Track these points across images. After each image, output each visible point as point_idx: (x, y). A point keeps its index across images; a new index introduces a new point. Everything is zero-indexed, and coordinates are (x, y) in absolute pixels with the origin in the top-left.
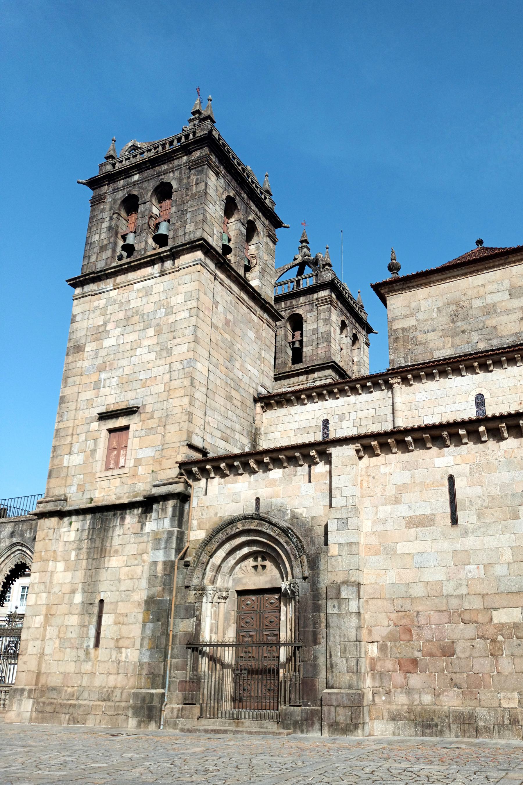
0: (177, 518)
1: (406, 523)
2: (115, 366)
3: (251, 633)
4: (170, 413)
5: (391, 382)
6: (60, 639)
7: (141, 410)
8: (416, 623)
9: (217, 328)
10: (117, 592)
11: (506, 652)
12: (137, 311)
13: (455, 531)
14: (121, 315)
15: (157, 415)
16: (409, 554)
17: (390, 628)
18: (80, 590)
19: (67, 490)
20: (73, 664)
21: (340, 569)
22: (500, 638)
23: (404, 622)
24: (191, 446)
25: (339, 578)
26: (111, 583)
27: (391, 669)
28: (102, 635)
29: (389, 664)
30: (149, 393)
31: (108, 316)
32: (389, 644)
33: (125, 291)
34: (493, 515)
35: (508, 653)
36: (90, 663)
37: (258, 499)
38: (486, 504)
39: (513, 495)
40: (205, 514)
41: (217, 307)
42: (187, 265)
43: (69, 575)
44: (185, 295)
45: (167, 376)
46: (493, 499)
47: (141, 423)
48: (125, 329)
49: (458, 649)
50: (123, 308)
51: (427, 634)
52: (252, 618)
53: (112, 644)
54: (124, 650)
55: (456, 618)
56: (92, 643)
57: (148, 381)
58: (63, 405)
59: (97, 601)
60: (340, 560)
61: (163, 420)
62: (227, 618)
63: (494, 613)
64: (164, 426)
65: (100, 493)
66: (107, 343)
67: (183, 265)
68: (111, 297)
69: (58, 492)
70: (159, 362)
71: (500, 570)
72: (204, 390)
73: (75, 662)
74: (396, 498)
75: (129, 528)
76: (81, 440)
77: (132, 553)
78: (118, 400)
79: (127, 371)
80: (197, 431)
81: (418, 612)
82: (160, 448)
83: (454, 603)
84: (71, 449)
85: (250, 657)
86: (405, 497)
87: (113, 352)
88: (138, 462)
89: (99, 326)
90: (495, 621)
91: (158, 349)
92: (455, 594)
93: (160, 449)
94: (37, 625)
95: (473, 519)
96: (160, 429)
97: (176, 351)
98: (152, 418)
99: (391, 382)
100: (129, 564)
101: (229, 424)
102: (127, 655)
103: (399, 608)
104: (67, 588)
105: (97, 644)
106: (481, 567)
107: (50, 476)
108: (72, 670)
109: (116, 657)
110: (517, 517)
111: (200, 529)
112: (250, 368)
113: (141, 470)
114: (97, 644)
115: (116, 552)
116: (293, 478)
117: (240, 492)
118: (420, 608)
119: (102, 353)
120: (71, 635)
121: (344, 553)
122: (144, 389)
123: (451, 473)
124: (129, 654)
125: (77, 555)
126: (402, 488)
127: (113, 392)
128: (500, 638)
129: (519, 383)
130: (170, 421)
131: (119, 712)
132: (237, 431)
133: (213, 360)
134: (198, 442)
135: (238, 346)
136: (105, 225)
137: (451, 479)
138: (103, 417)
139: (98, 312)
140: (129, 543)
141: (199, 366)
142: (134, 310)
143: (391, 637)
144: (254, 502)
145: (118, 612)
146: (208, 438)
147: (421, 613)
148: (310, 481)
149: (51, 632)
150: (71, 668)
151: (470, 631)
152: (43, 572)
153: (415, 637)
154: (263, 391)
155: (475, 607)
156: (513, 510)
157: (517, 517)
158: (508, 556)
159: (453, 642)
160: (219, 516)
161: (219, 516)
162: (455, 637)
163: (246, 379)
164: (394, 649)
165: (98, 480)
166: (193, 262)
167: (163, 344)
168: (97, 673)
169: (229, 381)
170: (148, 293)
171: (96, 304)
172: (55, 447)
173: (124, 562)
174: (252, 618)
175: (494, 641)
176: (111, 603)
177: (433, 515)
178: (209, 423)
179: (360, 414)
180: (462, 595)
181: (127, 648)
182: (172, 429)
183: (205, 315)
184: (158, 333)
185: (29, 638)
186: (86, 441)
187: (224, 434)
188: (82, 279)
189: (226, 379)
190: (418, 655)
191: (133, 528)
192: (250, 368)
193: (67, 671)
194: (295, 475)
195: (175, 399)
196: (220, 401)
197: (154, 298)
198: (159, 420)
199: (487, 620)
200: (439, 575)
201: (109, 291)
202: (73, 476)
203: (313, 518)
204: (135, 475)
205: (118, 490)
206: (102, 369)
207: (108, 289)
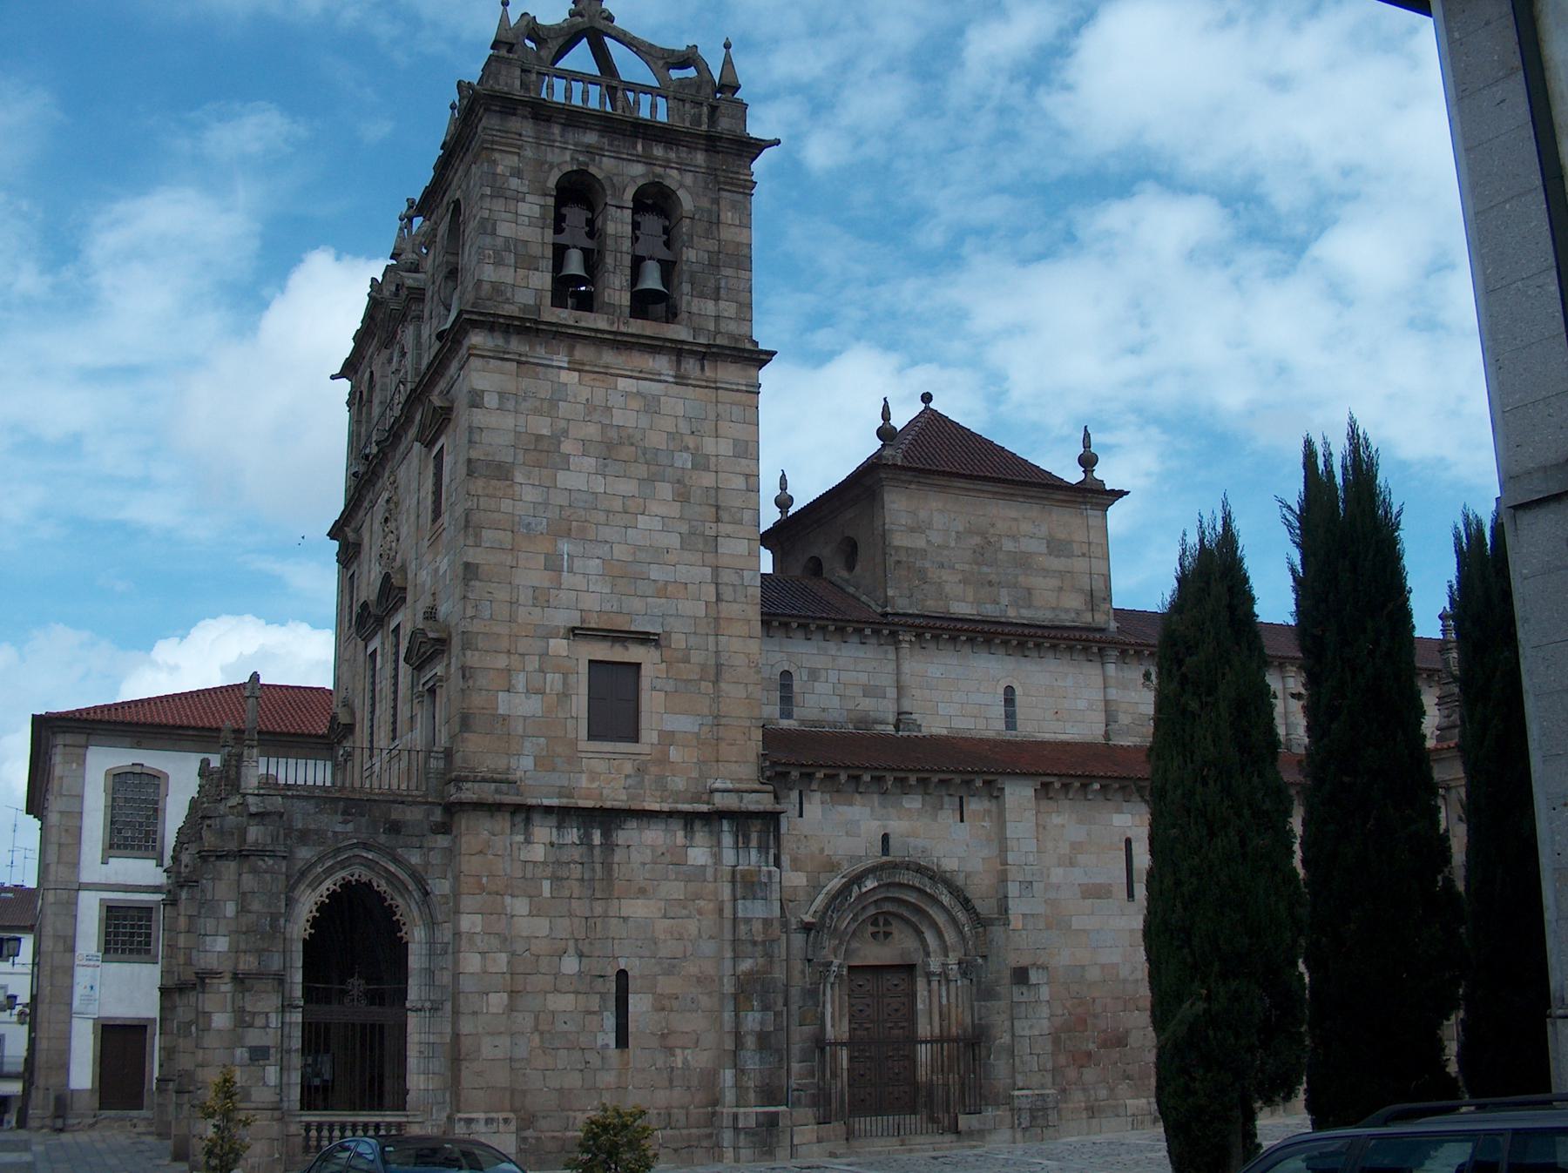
1: (1082, 893)
2: (591, 536)
4: (726, 663)
5: (901, 638)
10: (653, 960)
15: (696, 657)
16: (1084, 931)
18: (571, 950)
19: (513, 763)
20: (577, 1075)
26: (639, 943)
27: (1065, 1064)
30: (673, 612)
32: (1062, 1035)
33: (597, 384)
36: (614, 1073)
37: (885, 838)
42: (735, 387)
48: (606, 466)
49: (1131, 1040)
50: (596, 417)
52: (868, 1005)
54: (678, 1051)
59: (611, 972)
60: (1024, 936)
64: (716, 682)
65: (592, 780)
66: (564, 478)
67: (727, 383)
68: (566, 384)
70: (687, 556)
73: (581, 1071)
74: (1071, 858)
75: (663, 854)
77: (675, 896)
78: (607, 607)
79: (620, 552)
81: (1094, 1001)
84: (510, 681)
85: (868, 1057)
88: (668, 738)
91: (685, 528)
92: (1130, 978)
93: (710, 723)
94: (493, 1010)
97: (726, 547)
99: (901, 638)
100: (672, 915)
102: (686, 1059)
105: (622, 1040)
109: (665, 1062)
113: (674, 754)
114: (622, 1040)
116: (940, 812)
117: (858, 821)
122: (663, 600)
123: (1129, 835)
124: (689, 1058)
126: (1076, 847)
129: (1055, 683)
131: (692, 1143)
137: (1128, 842)
140: (666, 879)
145: (659, 991)
147: (1097, 1001)
148: (962, 821)
149: (525, 1021)
150: (574, 1080)
152: (491, 914)
160: (826, 853)
161: (826, 853)
164: (1068, 1042)
165: (583, 755)
166: (746, 385)
167: (695, 523)
168: (630, 1087)
170: (651, 406)
173: (660, 909)
176: (642, 977)
177: (1110, 884)
179: (845, 677)
180: (1137, 981)
181: (684, 1048)
184: (683, 497)
185: (480, 1029)
188: (501, 320)
190: (1092, 1046)
191: (672, 854)
193: (566, 1086)
194: (942, 808)
195: (734, 639)
198: (702, 670)
200: (1116, 958)
201: (560, 368)
202: (522, 736)
203: (968, 876)
204: (664, 760)
205: (630, 781)
207: (555, 363)
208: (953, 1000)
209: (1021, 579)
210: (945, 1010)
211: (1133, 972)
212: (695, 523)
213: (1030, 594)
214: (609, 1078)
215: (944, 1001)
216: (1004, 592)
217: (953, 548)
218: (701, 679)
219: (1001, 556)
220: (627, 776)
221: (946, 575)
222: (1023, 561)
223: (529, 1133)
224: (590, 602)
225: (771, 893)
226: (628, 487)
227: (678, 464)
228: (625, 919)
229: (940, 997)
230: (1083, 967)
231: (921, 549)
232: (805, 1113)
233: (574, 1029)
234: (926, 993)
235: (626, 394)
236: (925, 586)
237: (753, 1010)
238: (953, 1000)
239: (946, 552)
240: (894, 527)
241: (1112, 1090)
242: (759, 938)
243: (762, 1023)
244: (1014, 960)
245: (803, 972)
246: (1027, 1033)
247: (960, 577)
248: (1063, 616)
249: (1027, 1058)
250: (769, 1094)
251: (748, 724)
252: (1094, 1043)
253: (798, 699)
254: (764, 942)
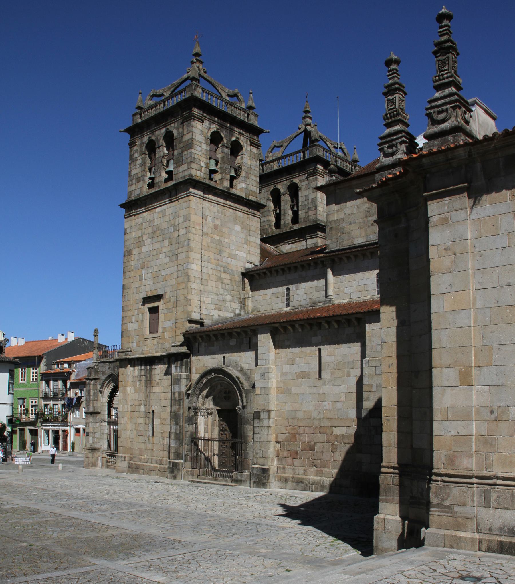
0: (184, 367)
3: (225, 433)
6: (136, 430)
7: (164, 297)
8: (298, 433)
9: (207, 234)
11: (338, 450)
12: (158, 227)
13: (320, 382)
14: (150, 230)
15: (172, 299)
16: (297, 394)
17: (287, 434)
18: (143, 404)
22: (336, 443)
23: (293, 432)
24: (191, 321)
25: (260, 408)
27: (286, 456)
28: (155, 430)
29: (285, 454)
30: (167, 285)
31: (144, 231)
32: (286, 443)
33: (152, 213)
34: (338, 373)
35: (339, 451)
36: (151, 444)
38: (336, 367)
39: (348, 362)
41: (206, 220)
43: (137, 395)
44: (183, 218)
45: (176, 274)
46: (339, 364)
47: (164, 305)
49: (316, 448)
50: (151, 225)
51: (303, 439)
53: (160, 435)
55: (317, 431)
56: (151, 433)
57: (166, 277)
58: (125, 290)
59: (151, 411)
61: (175, 303)
62: (213, 424)
63: (334, 429)
65: (148, 348)
66: (145, 249)
69: (127, 346)
70: (172, 264)
71: (339, 406)
72: (199, 281)
76: (135, 314)
79: (155, 269)
80: (195, 309)
82: (174, 321)
83: (316, 423)
86: (297, 360)
87: (147, 256)
88: (164, 329)
89: (139, 237)
90: (334, 433)
91: (170, 254)
95: (329, 376)
96: (174, 309)
98: (169, 302)
101: (221, 298)
103: (291, 425)
104: (137, 403)
107: (122, 336)
108: (143, 448)
110: (349, 376)
111: (196, 373)
112: (237, 252)
113: (166, 335)
115: (158, 384)
118: (300, 425)
119: (143, 256)
120: (140, 429)
121: (262, 393)
125: (140, 384)
127: (149, 283)
128: (336, 443)
130: (178, 305)
132: (228, 300)
133: (205, 258)
134: (196, 316)
135: (226, 240)
136: (139, 162)
138: (146, 300)
139: (138, 227)
141: (193, 266)
142: (157, 226)
143: (287, 440)
144: (223, 359)
146: (205, 312)
150: (142, 446)
151: (322, 438)
153: (298, 440)
154: (249, 266)
155: (326, 425)
156: (348, 371)
157: (349, 376)
158: (343, 398)
159: (315, 444)
160: (205, 366)
161: (205, 366)
162: (316, 441)
163: (234, 262)
164: (288, 446)
169: (219, 268)
171: (137, 221)
172: (123, 318)
175: (333, 444)
176: (158, 413)
177: (310, 372)
178: (204, 302)
182: (180, 309)
183: (196, 229)
184: (170, 244)
186: (138, 314)
187: (217, 306)
189: (216, 267)
192: (237, 252)
196: (212, 284)
197: (167, 219)
199: (331, 433)
204: (163, 338)
206: (143, 267)
211: (319, 414)
212: (173, 251)
214: (149, 446)
218: (173, 307)
220: (155, 345)
223: (131, 462)
224: (148, 288)
226: (157, 245)
227: (170, 231)
228: (154, 393)
230: (295, 411)
231: (342, 219)
232: (189, 464)
233: (142, 429)
235: (158, 213)
236: (344, 235)
239: (352, 217)
240: (330, 213)
241: (306, 470)
243: (176, 430)
244: (256, 407)
246: (258, 440)
247: (358, 226)
249: (258, 451)
250: (178, 456)
252: (299, 447)
253: (292, 298)
254: (178, 400)
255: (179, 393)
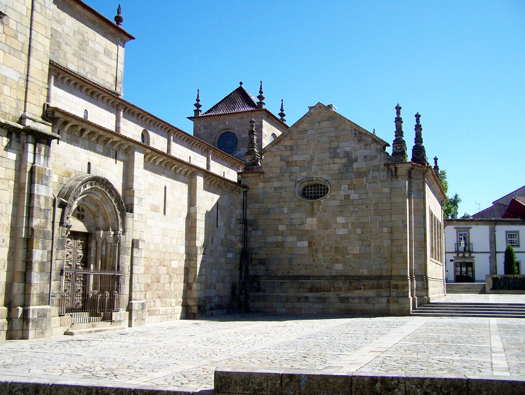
16: (150, 226)
21: (138, 230)
40: (57, 161)
90: (172, 266)
106: (170, 238)
137: (165, 188)
159: (160, 276)
174: (71, 252)
208: (108, 252)
209: (94, 62)
210: (104, 257)
213: (96, 70)
215: (104, 253)
216: (88, 65)
217: (71, 37)
219: (88, 48)
221: (67, 49)
222: (95, 54)
225: (49, 182)
229: (102, 251)
234: (95, 249)
236: (60, 51)
237: (39, 249)
238: (108, 252)
239: (69, 38)
242: (43, 207)
243: (42, 257)
245: (59, 230)
248: (106, 84)
251: (41, 85)
254: (45, 210)
255: (47, 198)
